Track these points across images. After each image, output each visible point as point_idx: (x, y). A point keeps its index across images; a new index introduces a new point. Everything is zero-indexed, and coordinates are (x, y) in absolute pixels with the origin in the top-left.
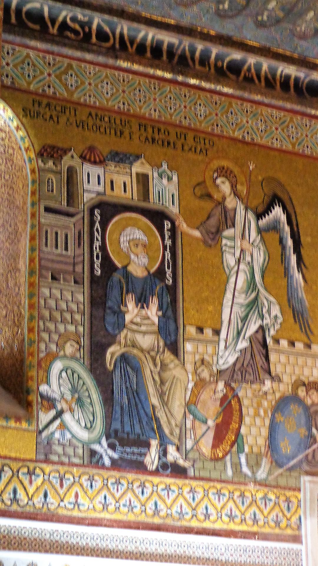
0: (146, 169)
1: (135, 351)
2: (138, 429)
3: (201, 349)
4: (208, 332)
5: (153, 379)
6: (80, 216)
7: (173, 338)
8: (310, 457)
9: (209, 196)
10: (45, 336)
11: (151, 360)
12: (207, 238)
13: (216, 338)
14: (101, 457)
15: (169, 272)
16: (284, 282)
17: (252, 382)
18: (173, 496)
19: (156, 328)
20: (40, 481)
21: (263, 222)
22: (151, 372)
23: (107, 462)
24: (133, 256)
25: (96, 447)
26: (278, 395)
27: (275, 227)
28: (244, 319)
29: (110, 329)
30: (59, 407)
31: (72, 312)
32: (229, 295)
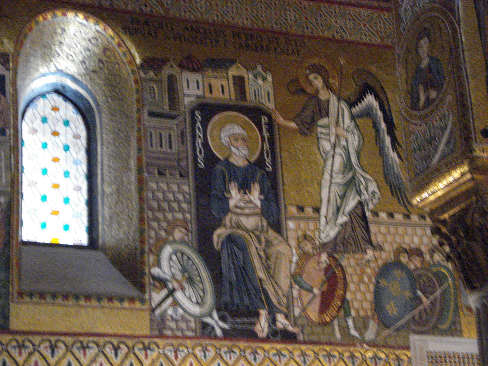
1: (240, 232)
2: (247, 302)
3: (303, 225)
4: (309, 211)
6: (181, 119)
8: (417, 318)
9: (303, 91)
11: (255, 239)
13: (317, 215)
14: (213, 328)
15: (268, 161)
17: (354, 252)
19: (259, 211)
20: (155, 354)
21: (356, 110)
22: (256, 248)
23: (219, 332)
24: (233, 149)
25: (208, 320)
26: (380, 262)
27: (368, 113)
28: (343, 197)
29: (215, 214)
30: (170, 286)
31: (178, 202)
32: (327, 176)
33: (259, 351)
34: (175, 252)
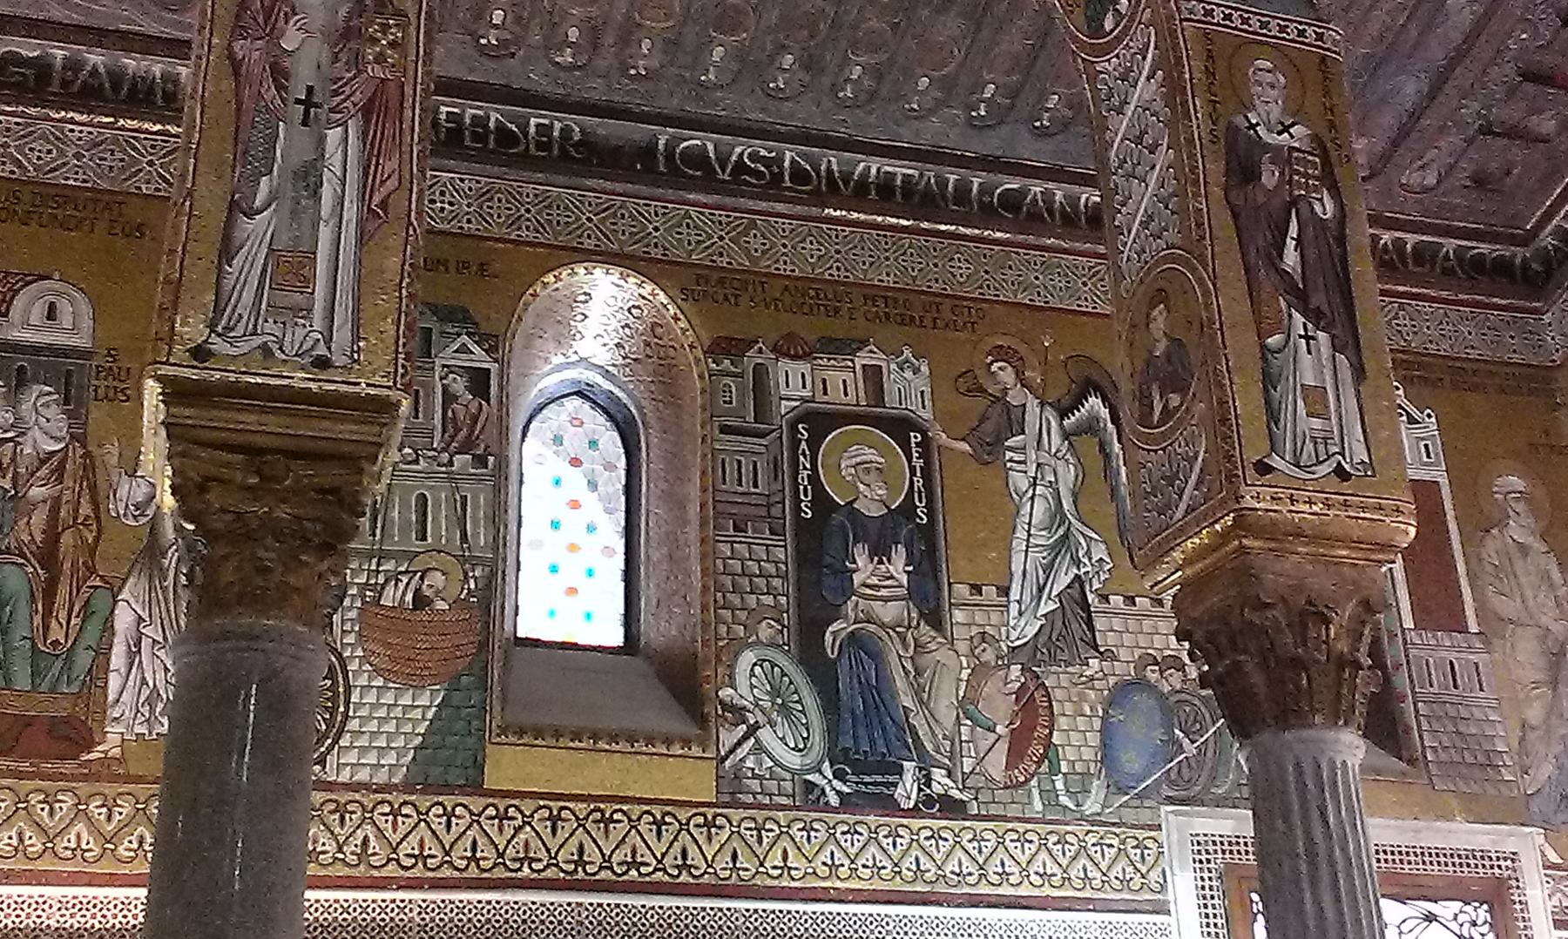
0: (878, 359)
3: (979, 617)
4: (990, 592)
5: (904, 667)
7: (932, 605)
10: (726, 613)
12: (980, 451)
14: (823, 791)
16: (1112, 509)
18: (945, 847)
22: (900, 656)
23: (834, 800)
26: (1112, 680)
27: (1091, 427)
28: (1048, 568)
29: (829, 598)
32: (1021, 534)
33: (901, 831)
34: (760, 662)
